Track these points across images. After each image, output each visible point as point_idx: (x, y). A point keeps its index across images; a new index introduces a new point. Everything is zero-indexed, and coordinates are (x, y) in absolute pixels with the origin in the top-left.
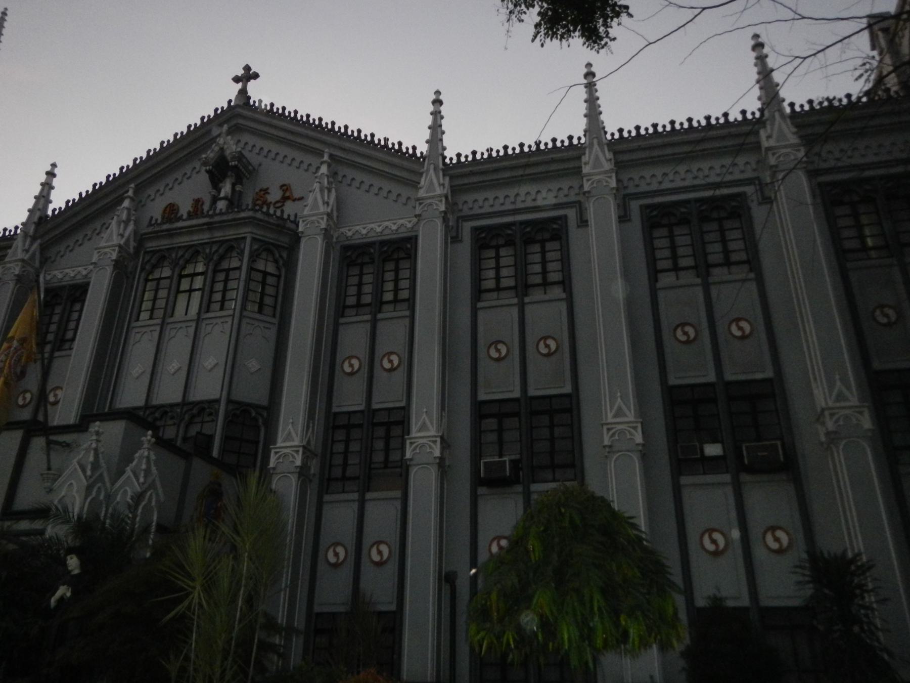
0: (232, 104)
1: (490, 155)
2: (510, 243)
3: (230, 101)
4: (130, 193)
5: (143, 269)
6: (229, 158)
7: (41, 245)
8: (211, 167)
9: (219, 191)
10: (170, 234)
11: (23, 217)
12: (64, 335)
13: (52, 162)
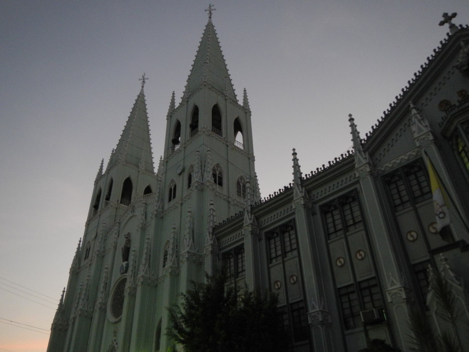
0: (450, 34)
3: (448, 34)
4: (412, 106)
7: (369, 154)
8: (467, 67)
12: (270, 256)
13: (348, 114)
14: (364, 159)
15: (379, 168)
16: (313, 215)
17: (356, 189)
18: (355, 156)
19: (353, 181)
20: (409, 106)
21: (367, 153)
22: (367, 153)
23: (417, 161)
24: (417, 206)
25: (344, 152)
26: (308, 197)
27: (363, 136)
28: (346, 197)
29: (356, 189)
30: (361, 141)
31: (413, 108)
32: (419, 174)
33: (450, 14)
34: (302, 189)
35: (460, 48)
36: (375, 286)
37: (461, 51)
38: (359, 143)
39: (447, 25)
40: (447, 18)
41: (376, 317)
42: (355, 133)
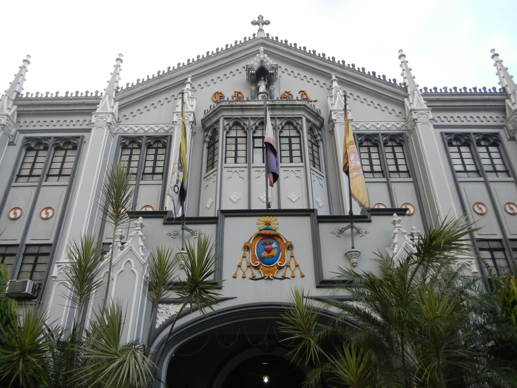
0: (256, 36)
1: (446, 91)
2: (467, 144)
3: (254, 35)
4: (189, 80)
5: (224, 129)
6: (268, 68)
7: (119, 106)
9: (258, 88)
10: (243, 108)
11: (106, 85)
14: (110, 107)
15: (121, 126)
16: (9, 145)
17: (83, 137)
18: (102, 100)
19: (84, 127)
20: (187, 79)
21: (117, 104)
22: (117, 104)
23: (165, 137)
24: (142, 182)
25: (92, 91)
26: (15, 120)
27: (122, 84)
28: (67, 141)
29: (83, 137)
30: (118, 88)
31: (189, 83)
32: (160, 151)
33: (264, 20)
34: (12, 107)
35: (258, 52)
36: (47, 254)
37: (258, 55)
38: (115, 88)
39: (257, 27)
40: (260, 22)
41: (28, 290)
42: (115, 74)
